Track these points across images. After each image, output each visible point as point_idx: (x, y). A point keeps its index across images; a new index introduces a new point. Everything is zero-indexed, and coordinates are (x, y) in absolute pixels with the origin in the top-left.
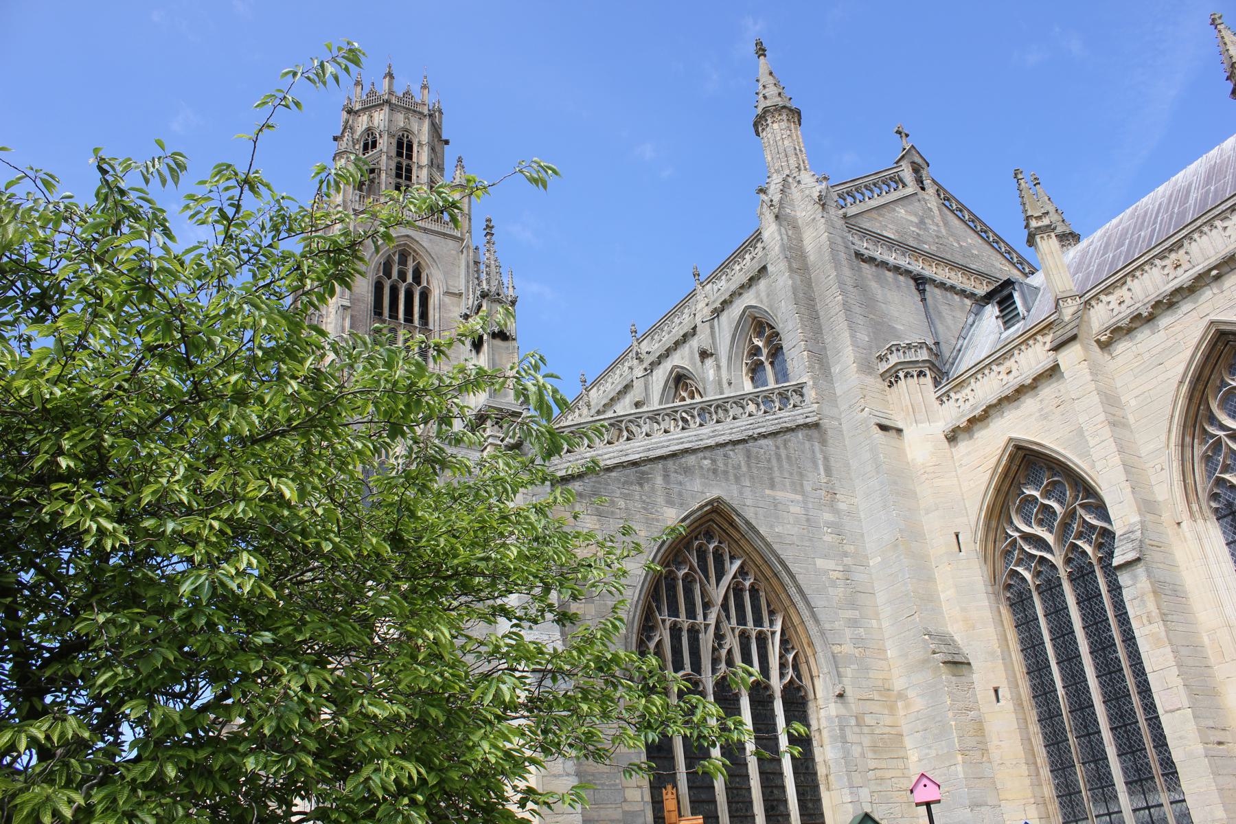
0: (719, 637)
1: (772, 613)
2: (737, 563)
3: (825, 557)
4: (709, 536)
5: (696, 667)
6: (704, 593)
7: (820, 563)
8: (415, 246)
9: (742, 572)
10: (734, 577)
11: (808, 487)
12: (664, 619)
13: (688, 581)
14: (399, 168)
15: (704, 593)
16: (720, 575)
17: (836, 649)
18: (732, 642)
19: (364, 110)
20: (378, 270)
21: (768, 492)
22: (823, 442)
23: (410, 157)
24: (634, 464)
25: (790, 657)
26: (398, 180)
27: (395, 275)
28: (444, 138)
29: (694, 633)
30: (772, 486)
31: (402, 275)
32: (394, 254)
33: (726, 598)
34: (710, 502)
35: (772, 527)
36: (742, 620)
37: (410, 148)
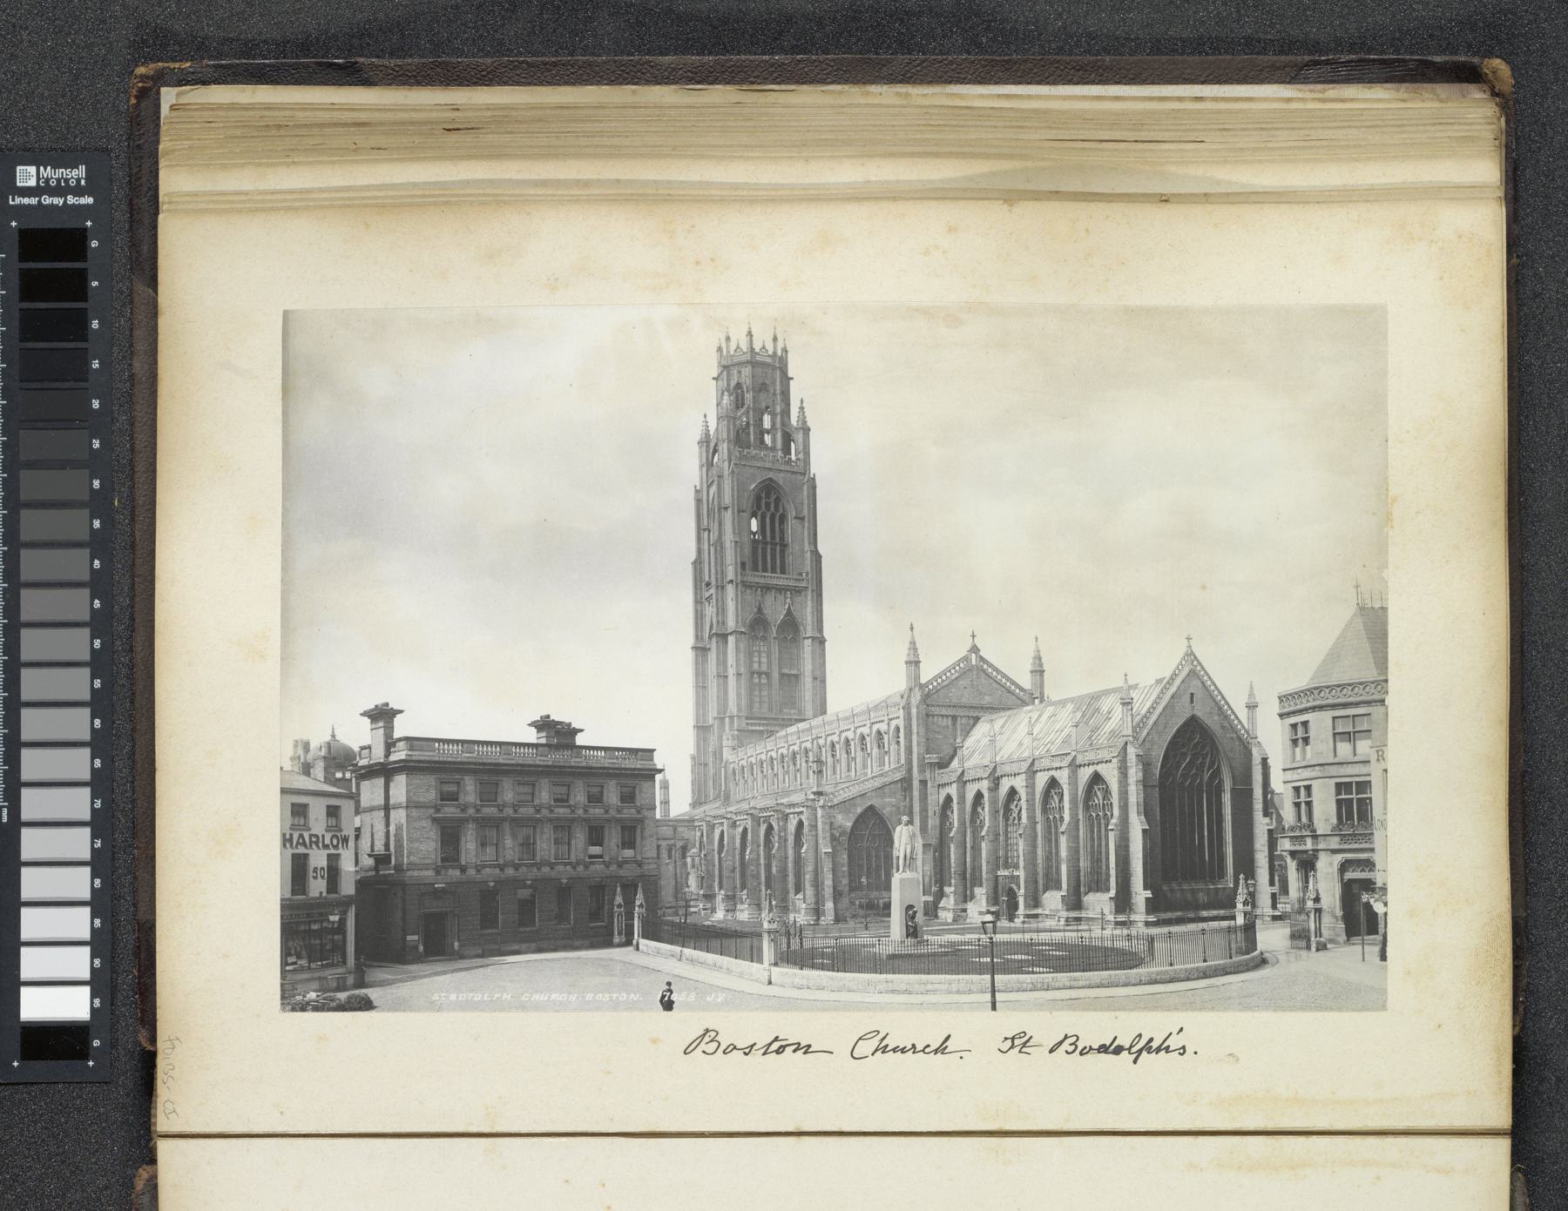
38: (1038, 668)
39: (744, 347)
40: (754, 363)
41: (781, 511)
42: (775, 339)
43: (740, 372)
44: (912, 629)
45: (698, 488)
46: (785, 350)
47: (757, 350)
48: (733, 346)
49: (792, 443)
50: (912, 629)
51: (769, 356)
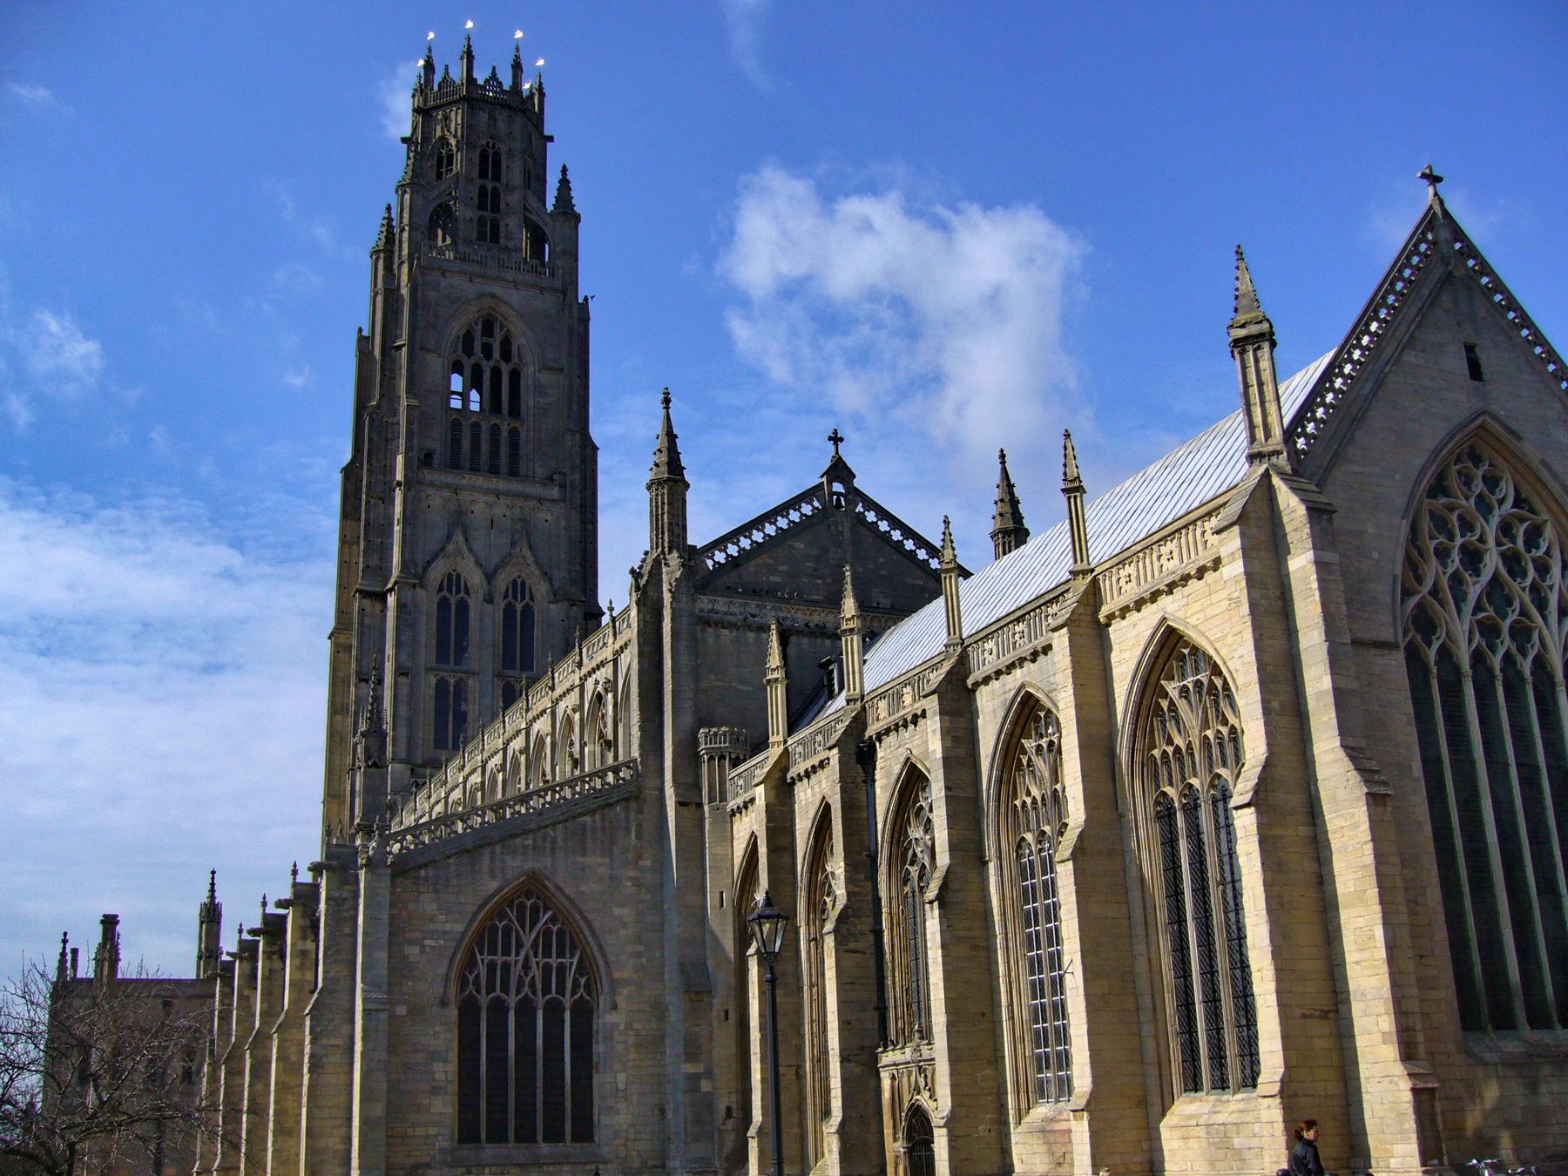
0: (526, 966)
1: (573, 947)
2: (549, 914)
3: (622, 905)
4: (529, 895)
5: (505, 989)
6: (518, 938)
7: (617, 911)
8: (503, 309)
9: (553, 919)
10: (546, 923)
11: (616, 851)
12: (483, 959)
13: (507, 931)
14: (483, 192)
17: (616, 975)
18: (536, 972)
20: (457, 347)
21: (580, 859)
22: (640, 811)
23: (496, 177)
24: (468, 851)
25: (583, 981)
26: (481, 212)
27: (477, 347)
28: (547, 133)
29: (506, 967)
30: (583, 855)
31: (487, 350)
32: (476, 325)
33: (536, 940)
36: (547, 954)
37: (497, 163)
38: (1011, 525)
40: (473, 97)
42: (517, 67)
43: (446, 118)
44: (667, 401)
45: (366, 333)
47: (481, 82)
48: (438, 78)
49: (547, 246)
50: (667, 401)
51: (503, 91)
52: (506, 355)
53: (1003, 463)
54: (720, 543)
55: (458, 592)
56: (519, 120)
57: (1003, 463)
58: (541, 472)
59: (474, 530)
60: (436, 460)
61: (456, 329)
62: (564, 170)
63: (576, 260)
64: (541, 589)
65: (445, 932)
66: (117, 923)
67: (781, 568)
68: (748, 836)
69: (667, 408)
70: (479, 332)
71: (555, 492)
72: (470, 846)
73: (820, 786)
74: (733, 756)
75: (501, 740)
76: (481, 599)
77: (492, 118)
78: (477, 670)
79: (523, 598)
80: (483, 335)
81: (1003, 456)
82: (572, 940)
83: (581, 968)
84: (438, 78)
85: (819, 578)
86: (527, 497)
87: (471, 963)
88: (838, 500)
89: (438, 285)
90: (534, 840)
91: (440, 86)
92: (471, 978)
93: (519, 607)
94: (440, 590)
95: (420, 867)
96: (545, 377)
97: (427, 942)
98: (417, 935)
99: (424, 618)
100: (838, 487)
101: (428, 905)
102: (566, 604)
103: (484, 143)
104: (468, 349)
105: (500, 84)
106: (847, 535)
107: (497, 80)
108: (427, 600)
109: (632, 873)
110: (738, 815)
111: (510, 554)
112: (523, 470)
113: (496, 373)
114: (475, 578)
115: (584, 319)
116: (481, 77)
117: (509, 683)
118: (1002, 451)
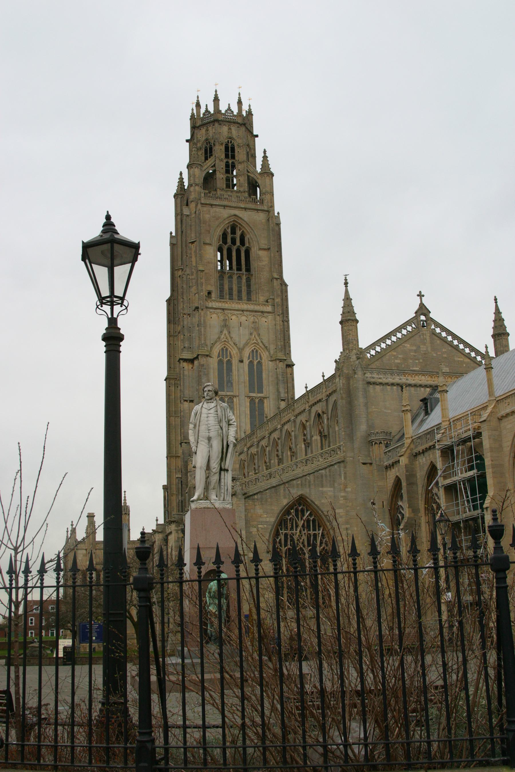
1: (319, 527)
2: (309, 512)
3: (340, 508)
4: (300, 504)
6: (296, 523)
9: (310, 515)
10: (307, 517)
11: (336, 485)
14: (227, 165)
15: (296, 523)
16: (303, 515)
18: (304, 537)
19: (203, 125)
20: (219, 240)
21: (320, 489)
22: (345, 467)
23: (233, 157)
24: (274, 487)
27: (229, 240)
28: (255, 133)
30: (322, 487)
31: (234, 242)
32: (228, 228)
33: (304, 524)
34: (299, 496)
35: (320, 501)
39: (211, 109)
41: (247, 245)
42: (240, 102)
43: (207, 130)
44: (346, 284)
46: (250, 113)
47: (223, 112)
48: (203, 110)
49: (258, 189)
51: (234, 116)
52: (242, 242)
53: (496, 302)
54: (372, 346)
55: (226, 358)
56: (243, 129)
57: (496, 302)
58: (262, 299)
59: (233, 328)
60: (213, 295)
61: (219, 232)
62: (265, 152)
63: (273, 195)
64: (265, 355)
65: (267, 522)
66: (94, 516)
67: (400, 356)
68: (394, 477)
69: (346, 287)
70: (230, 233)
71: (269, 309)
72: (274, 485)
73: (429, 457)
74: (385, 442)
75: (267, 432)
76: (237, 361)
77: (230, 129)
78: (237, 395)
79: (257, 359)
80: (231, 234)
81: (496, 299)
82: (319, 524)
83: (323, 535)
84: (203, 110)
85: (416, 359)
86: (256, 311)
87: (277, 534)
88: (423, 323)
89: (209, 211)
90: (301, 482)
91: (204, 114)
92: (278, 540)
93: (255, 363)
94: (219, 356)
95: (255, 494)
96: (261, 253)
97: (260, 526)
98: (255, 523)
99: (212, 371)
100: (423, 318)
101: (259, 510)
102: (278, 362)
103: (227, 141)
104: (225, 241)
105: (232, 112)
106: (428, 338)
107: (231, 110)
108: (213, 362)
109: (343, 494)
110: (389, 469)
111: (250, 339)
112: (253, 297)
113: (238, 251)
114: (234, 352)
115: (278, 225)
116: (223, 108)
117: (252, 399)
118: (495, 297)
